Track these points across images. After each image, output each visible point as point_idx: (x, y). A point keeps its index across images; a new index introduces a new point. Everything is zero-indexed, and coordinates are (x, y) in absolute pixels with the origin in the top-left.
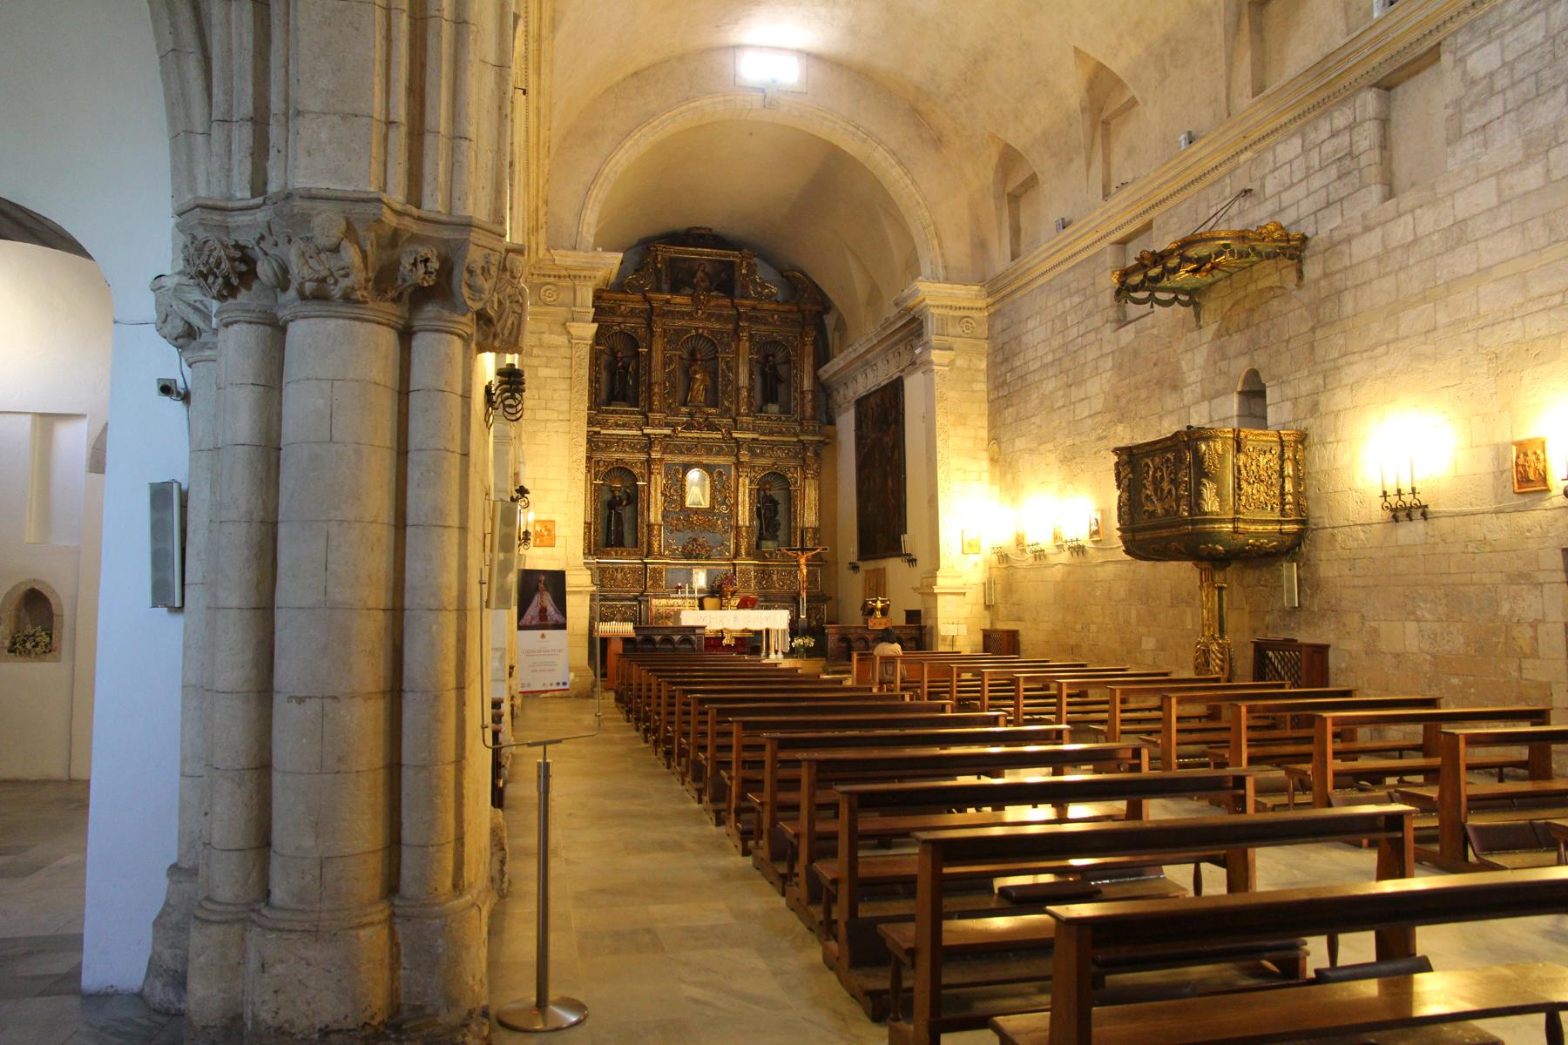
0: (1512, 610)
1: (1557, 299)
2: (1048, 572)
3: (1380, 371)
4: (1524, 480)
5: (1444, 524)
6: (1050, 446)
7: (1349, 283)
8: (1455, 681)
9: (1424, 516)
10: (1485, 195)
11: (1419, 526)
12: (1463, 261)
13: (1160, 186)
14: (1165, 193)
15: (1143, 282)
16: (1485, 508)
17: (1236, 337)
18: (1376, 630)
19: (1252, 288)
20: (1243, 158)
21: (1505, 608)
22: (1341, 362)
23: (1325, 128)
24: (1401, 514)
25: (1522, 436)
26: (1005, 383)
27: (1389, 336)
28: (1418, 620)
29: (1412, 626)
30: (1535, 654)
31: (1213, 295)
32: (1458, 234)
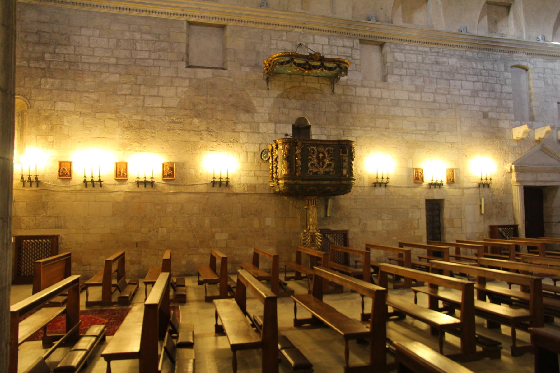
0: (412, 216)
1: (424, 132)
2: (105, 196)
3: (368, 136)
4: (417, 178)
5: (392, 190)
6: (113, 116)
7: (355, 102)
8: (394, 238)
9: (386, 186)
10: (403, 95)
11: (383, 189)
12: (397, 111)
13: (245, 14)
14: (246, 19)
15: (305, 64)
16: (404, 186)
17: (293, 101)
18: (366, 224)
19: (303, 84)
20: (296, 30)
21: (410, 215)
22: (351, 128)
23: (340, 42)
24: (482, 186)
25: (415, 167)
26: (43, 59)
27: (372, 125)
28: (382, 220)
29: (380, 222)
30: (418, 228)
31: (278, 78)
32: (396, 103)
